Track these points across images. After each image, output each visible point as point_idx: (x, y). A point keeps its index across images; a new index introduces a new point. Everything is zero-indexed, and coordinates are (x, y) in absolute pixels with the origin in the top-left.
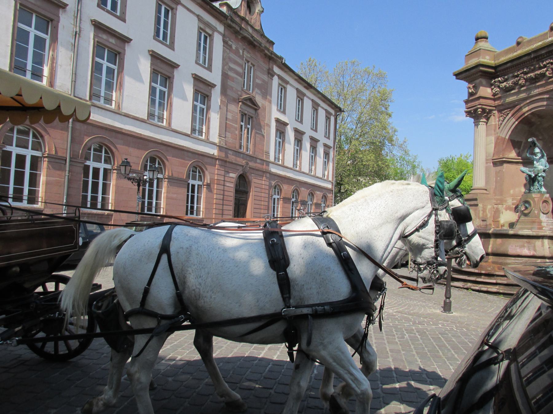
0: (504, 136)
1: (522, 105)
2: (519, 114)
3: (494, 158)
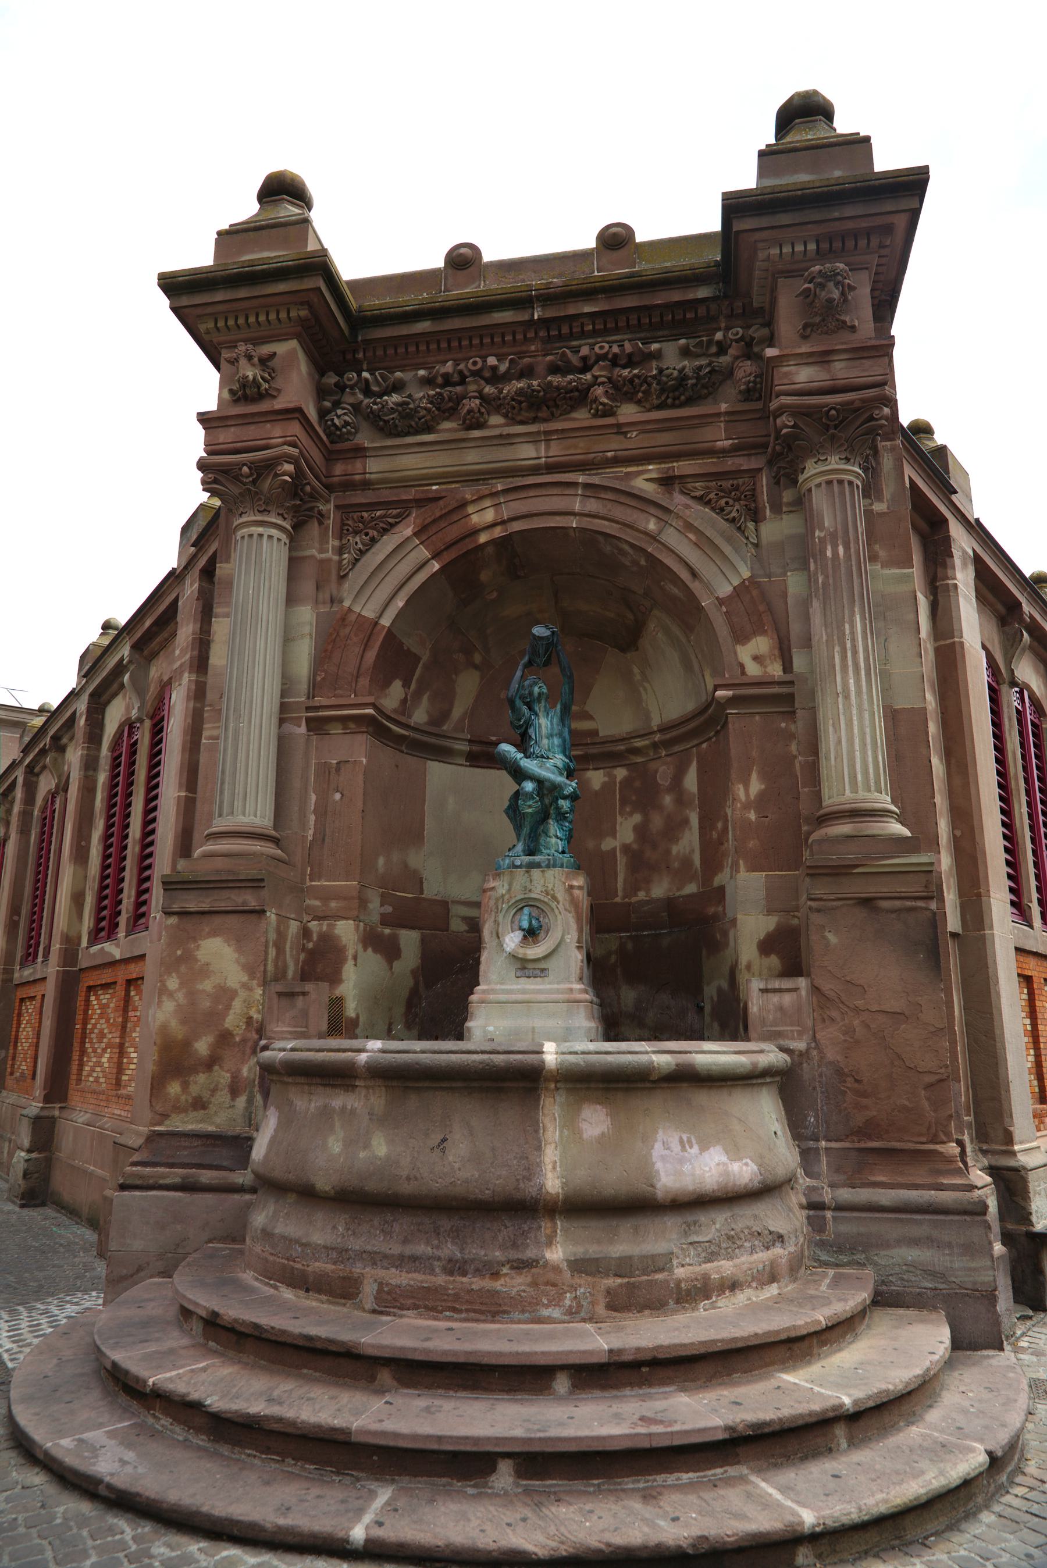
0: (369, 613)
2: (453, 532)
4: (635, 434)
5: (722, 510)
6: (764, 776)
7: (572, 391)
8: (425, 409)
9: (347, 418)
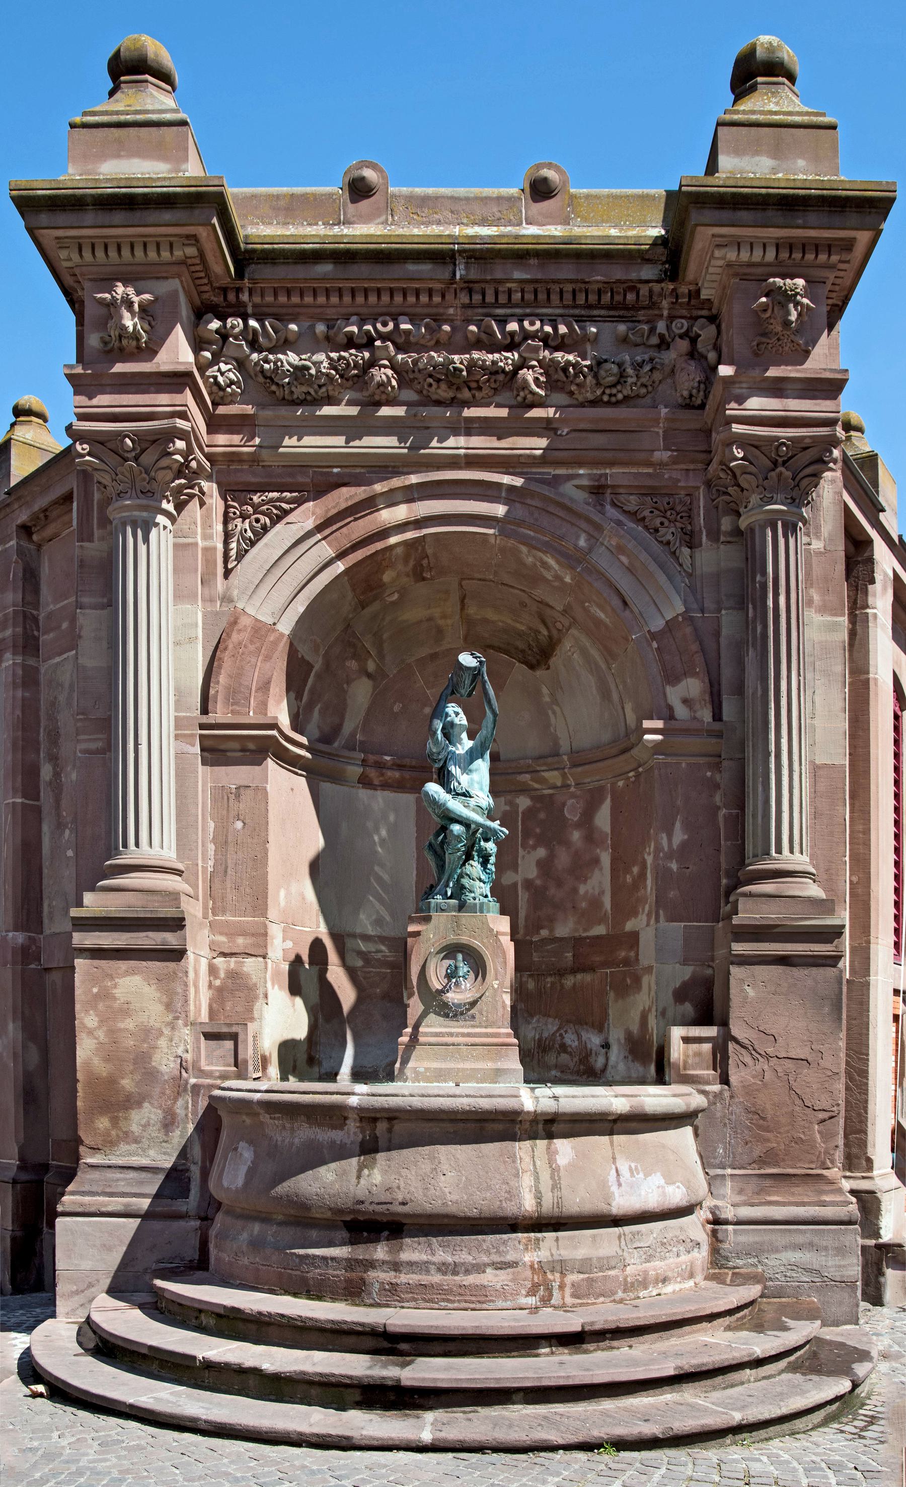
1: (379, 488)
3: (219, 714)
4: (566, 431)
5: (657, 531)
6: (686, 827)
7: (496, 373)
8: (327, 375)
9: (231, 376)
